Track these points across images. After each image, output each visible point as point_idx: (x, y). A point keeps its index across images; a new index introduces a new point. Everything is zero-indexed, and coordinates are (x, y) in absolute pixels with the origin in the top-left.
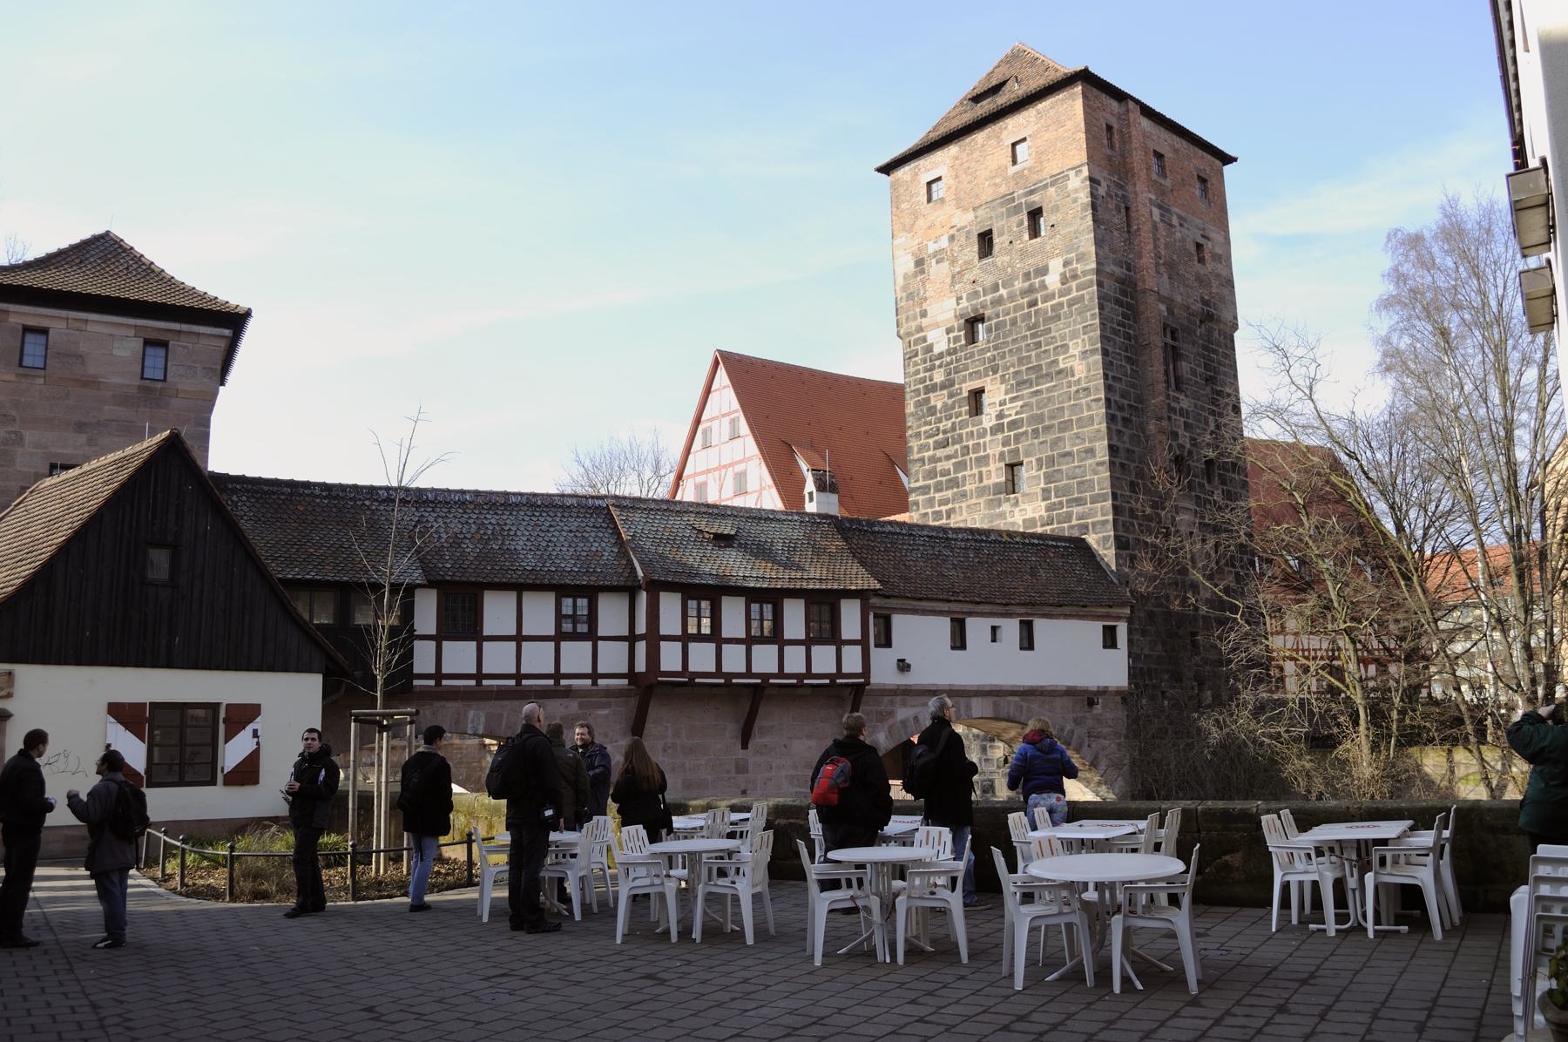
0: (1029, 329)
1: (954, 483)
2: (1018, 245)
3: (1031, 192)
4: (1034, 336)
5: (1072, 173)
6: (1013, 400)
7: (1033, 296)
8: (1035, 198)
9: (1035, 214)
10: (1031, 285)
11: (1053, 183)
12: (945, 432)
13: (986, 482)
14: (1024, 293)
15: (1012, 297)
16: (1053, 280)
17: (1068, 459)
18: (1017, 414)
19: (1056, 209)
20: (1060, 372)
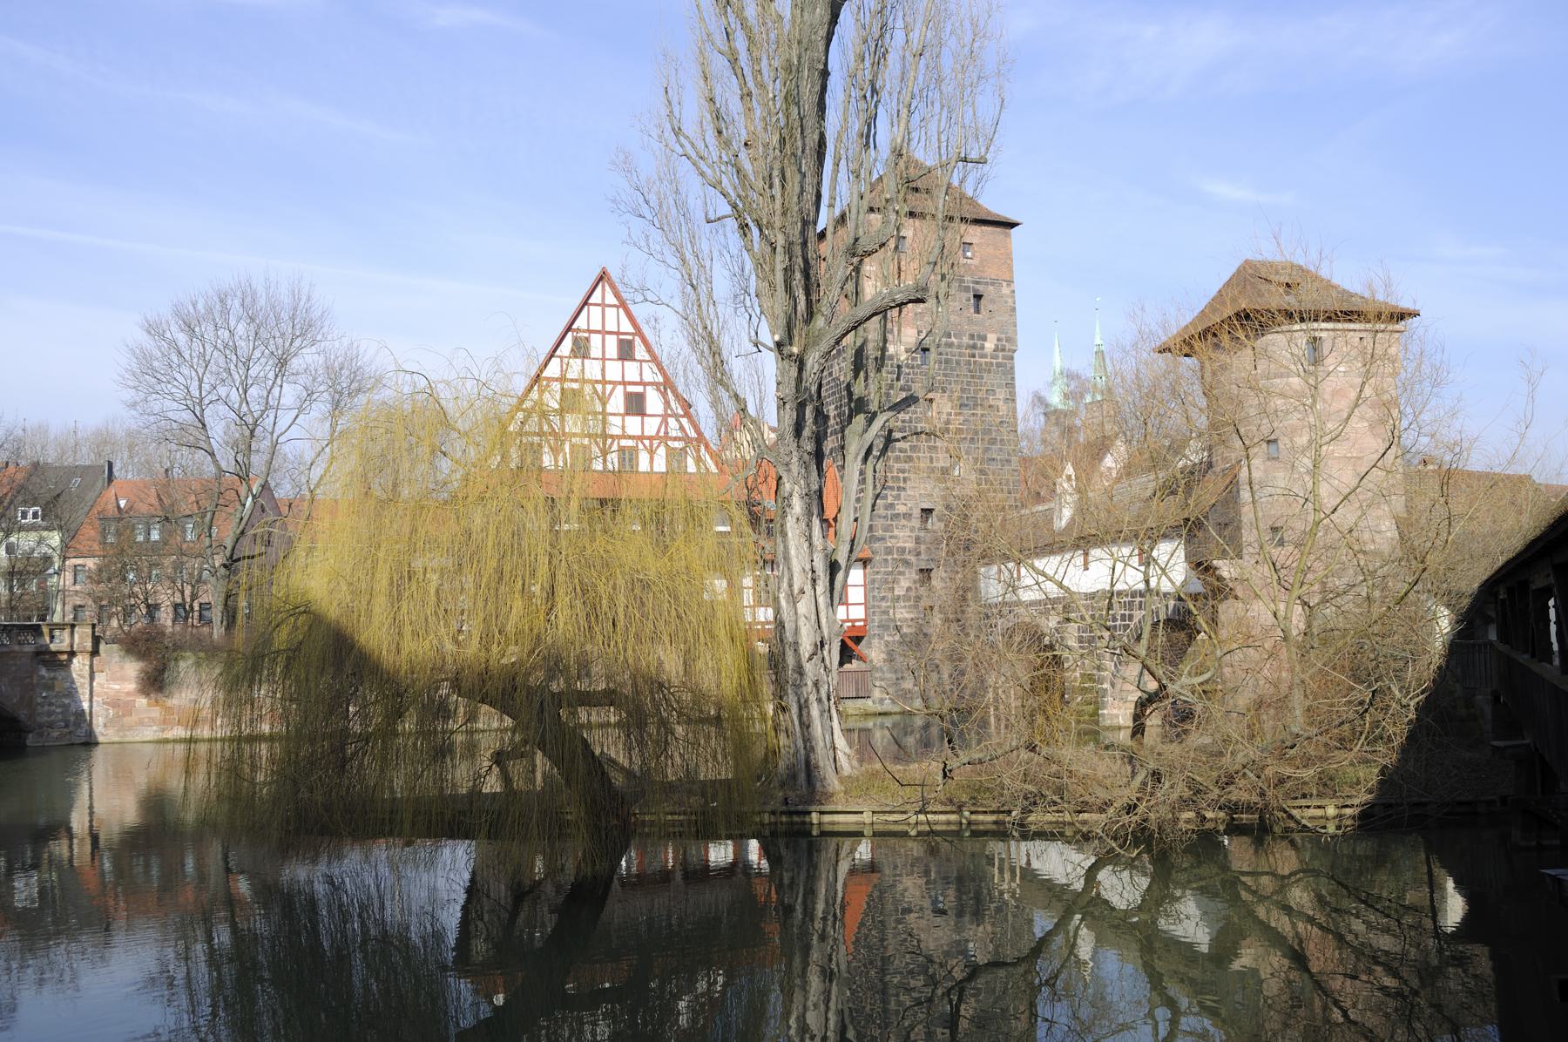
0: (970, 371)
1: (910, 459)
2: (965, 313)
3: (977, 283)
4: (972, 377)
5: (1005, 284)
6: (956, 414)
7: (974, 351)
8: (980, 288)
9: (978, 297)
10: (975, 344)
11: (992, 284)
12: (903, 421)
13: (935, 464)
14: (968, 347)
15: (959, 347)
16: (989, 346)
17: (994, 463)
18: (960, 424)
19: (992, 301)
20: (990, 406)
